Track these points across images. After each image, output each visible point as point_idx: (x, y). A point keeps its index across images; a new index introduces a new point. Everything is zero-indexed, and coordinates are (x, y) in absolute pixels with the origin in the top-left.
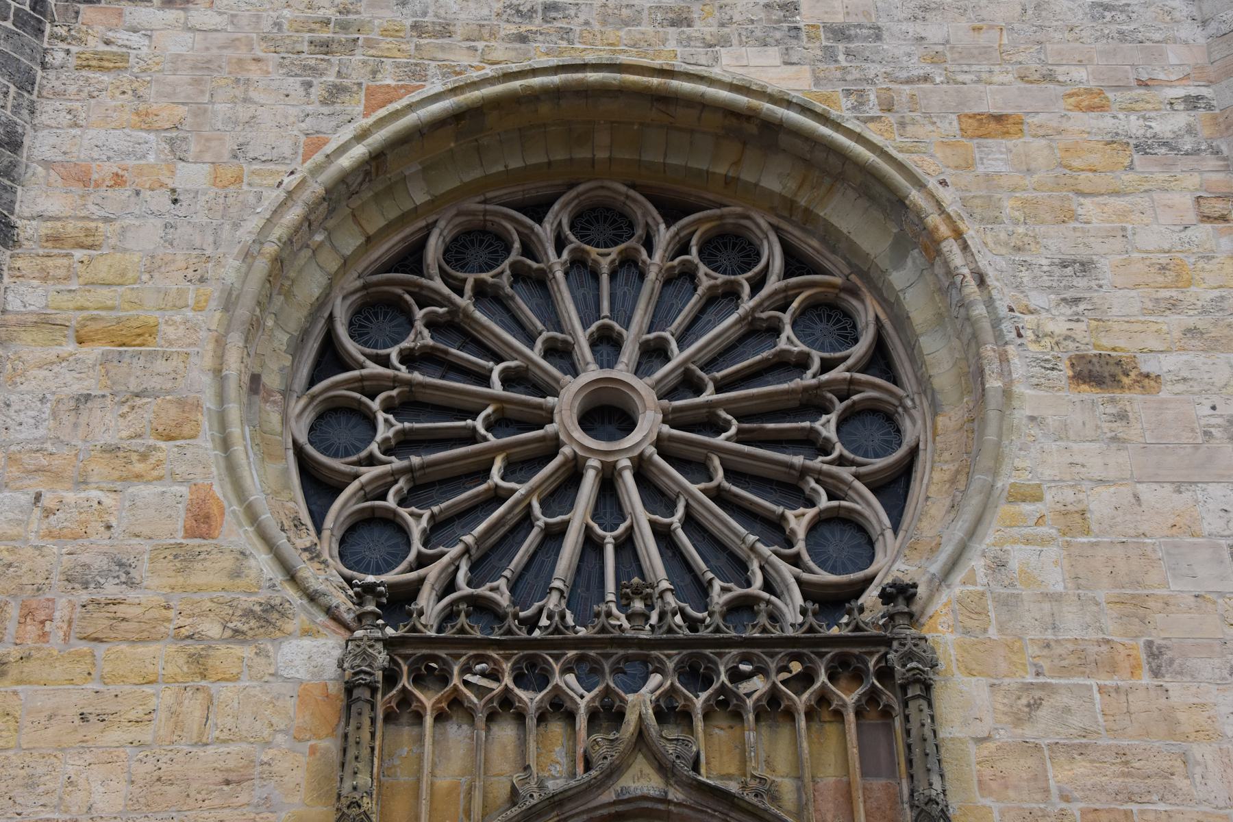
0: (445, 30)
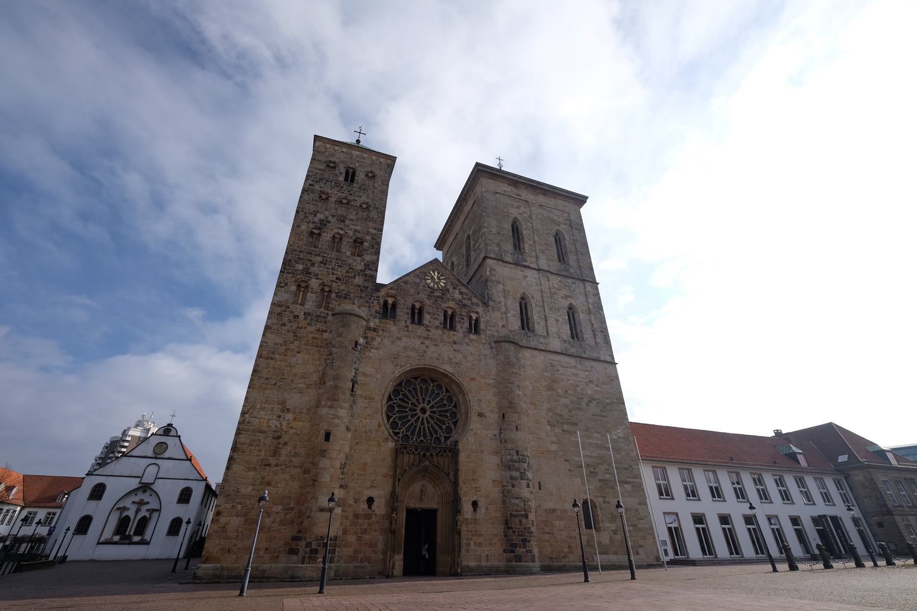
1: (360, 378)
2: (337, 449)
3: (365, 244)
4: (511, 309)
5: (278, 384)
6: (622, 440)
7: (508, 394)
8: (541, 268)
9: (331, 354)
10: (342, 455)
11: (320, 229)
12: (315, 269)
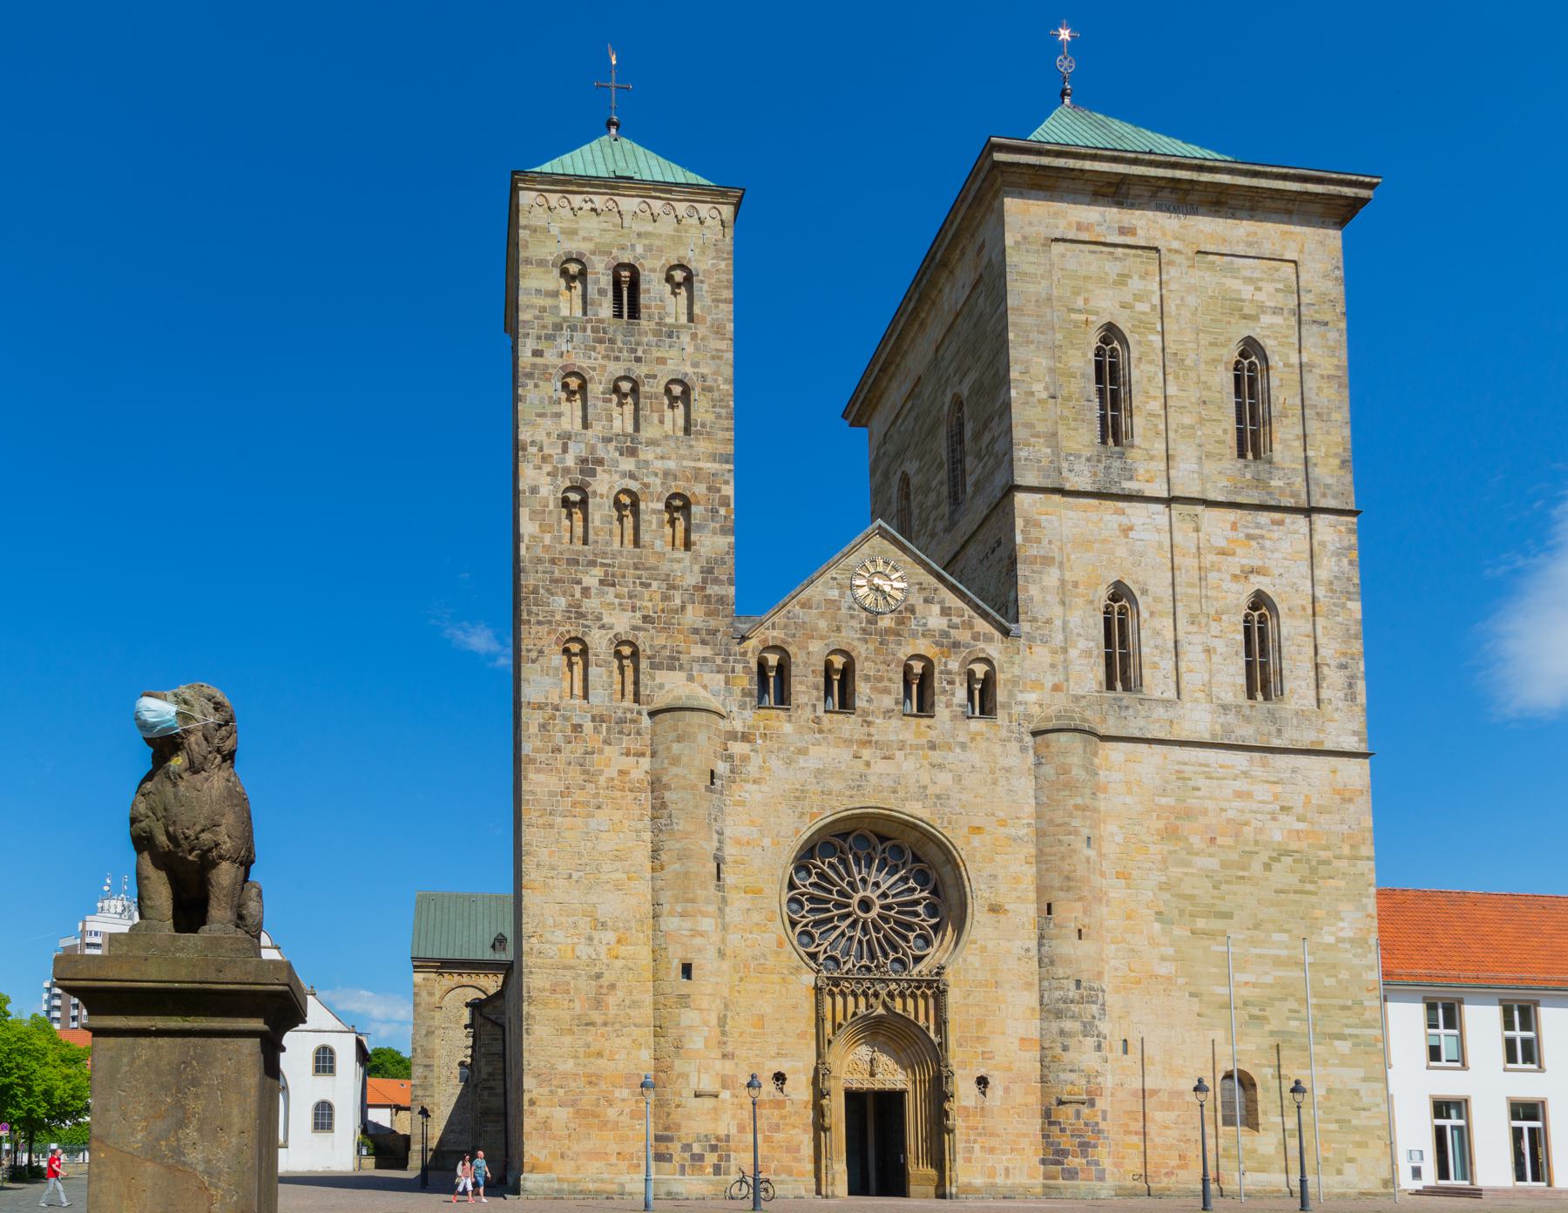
0: (830, 793)
1: (730, 851)
2: (708, 992)
3: (694, 509)
4: (1079, 635)
5: (575, 875)
6: (1348, 946)
7: (1063, 859)
8: (1177, 493)
10: (719, 1004)
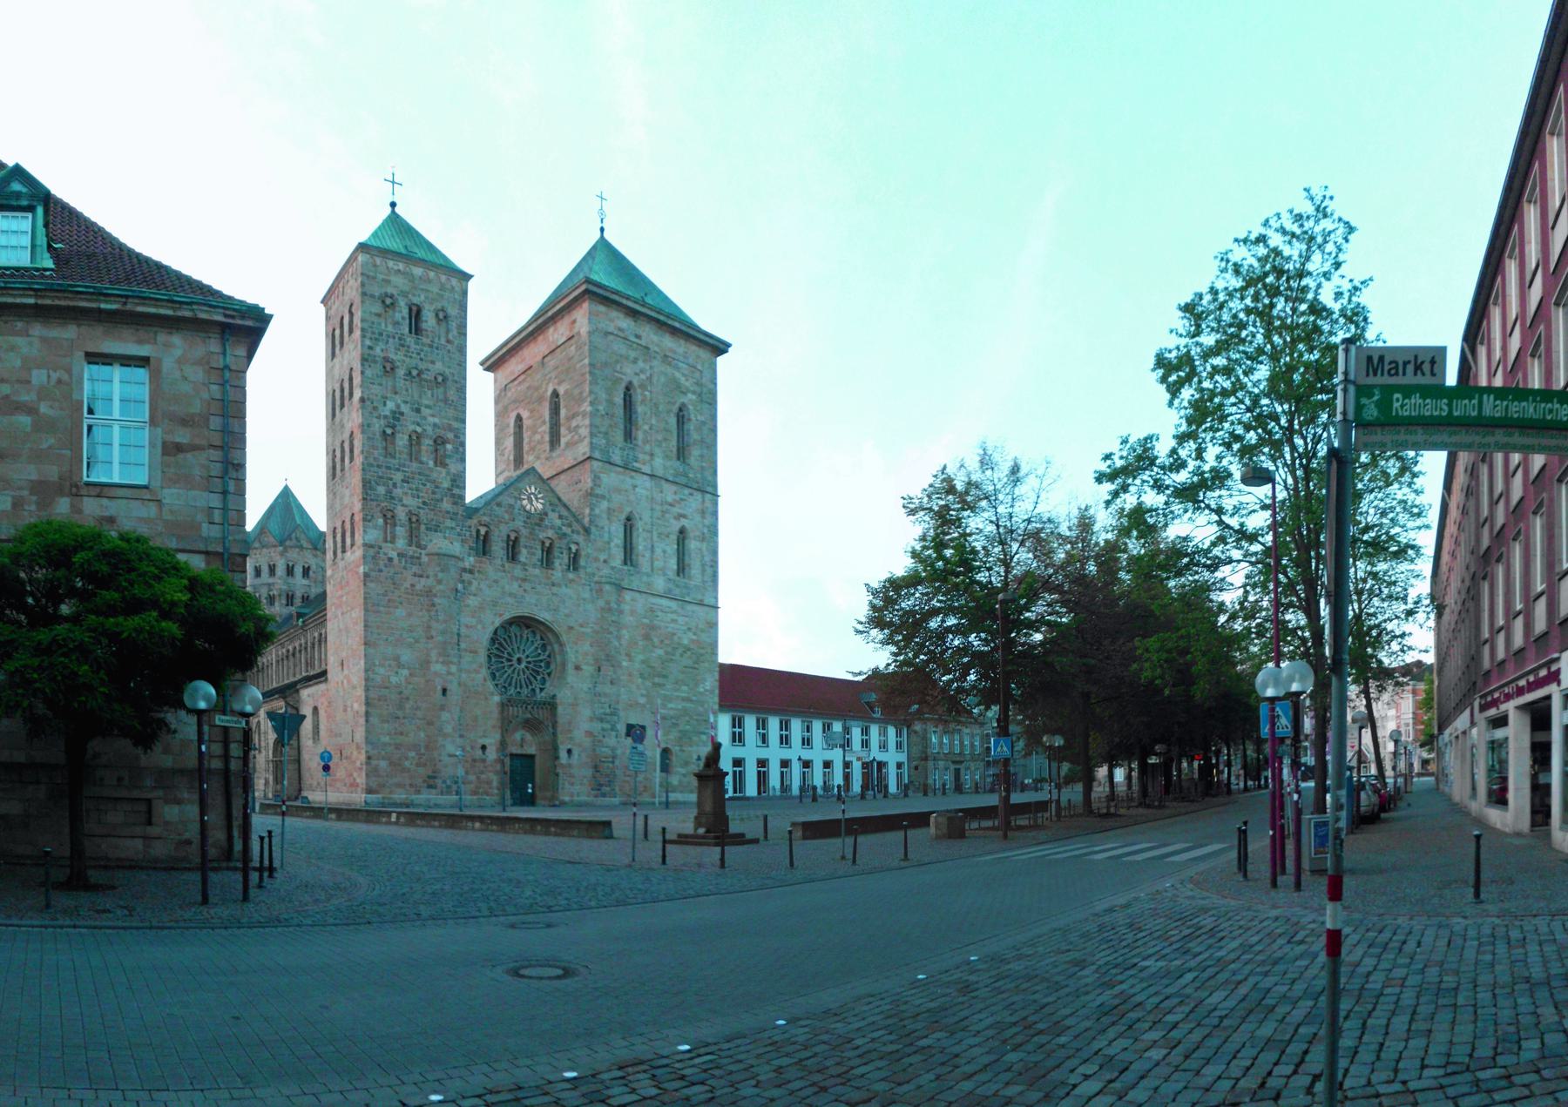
1: (463, 630)
9: (433, 605)
11: (393, 427)
12: (398, 492)
